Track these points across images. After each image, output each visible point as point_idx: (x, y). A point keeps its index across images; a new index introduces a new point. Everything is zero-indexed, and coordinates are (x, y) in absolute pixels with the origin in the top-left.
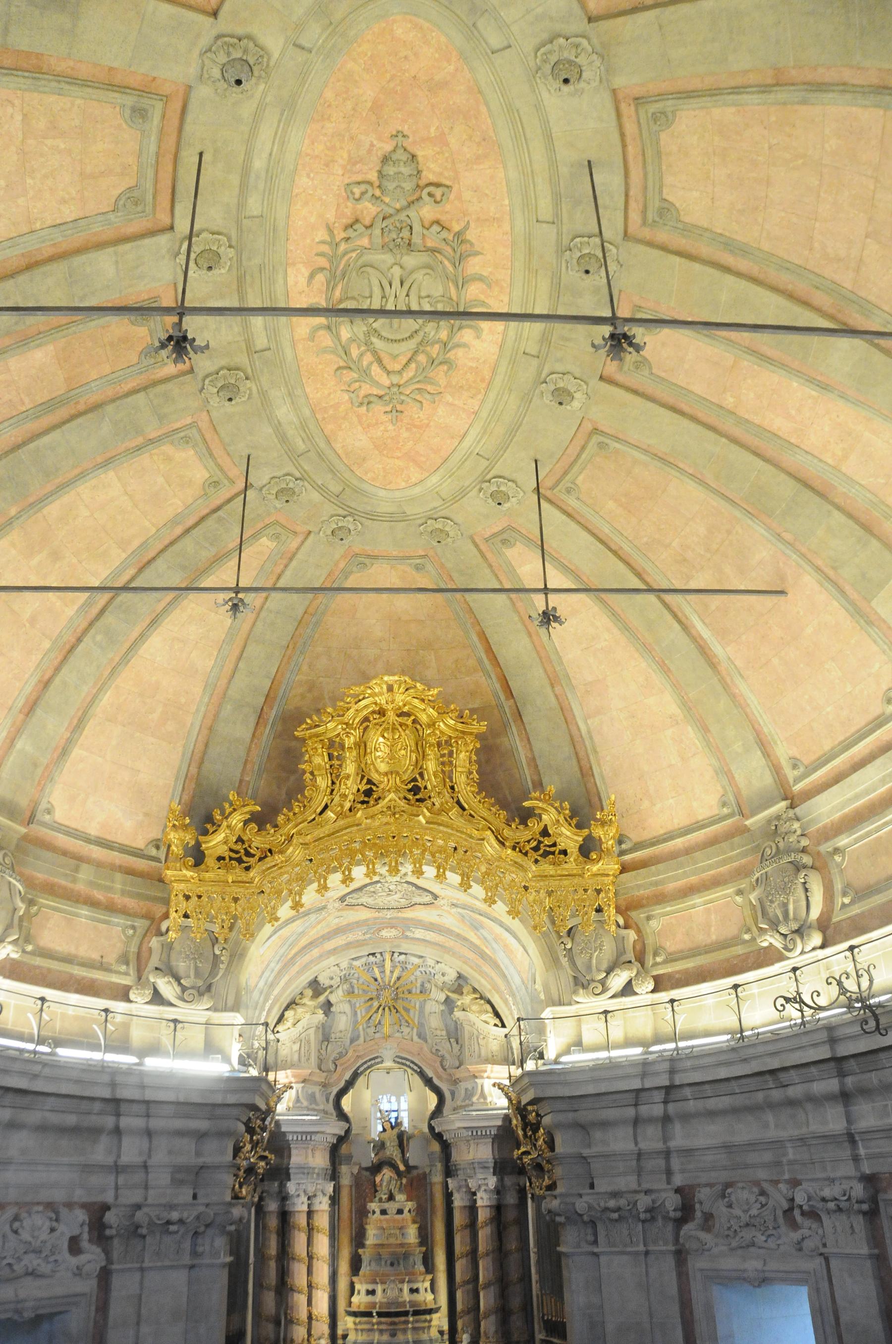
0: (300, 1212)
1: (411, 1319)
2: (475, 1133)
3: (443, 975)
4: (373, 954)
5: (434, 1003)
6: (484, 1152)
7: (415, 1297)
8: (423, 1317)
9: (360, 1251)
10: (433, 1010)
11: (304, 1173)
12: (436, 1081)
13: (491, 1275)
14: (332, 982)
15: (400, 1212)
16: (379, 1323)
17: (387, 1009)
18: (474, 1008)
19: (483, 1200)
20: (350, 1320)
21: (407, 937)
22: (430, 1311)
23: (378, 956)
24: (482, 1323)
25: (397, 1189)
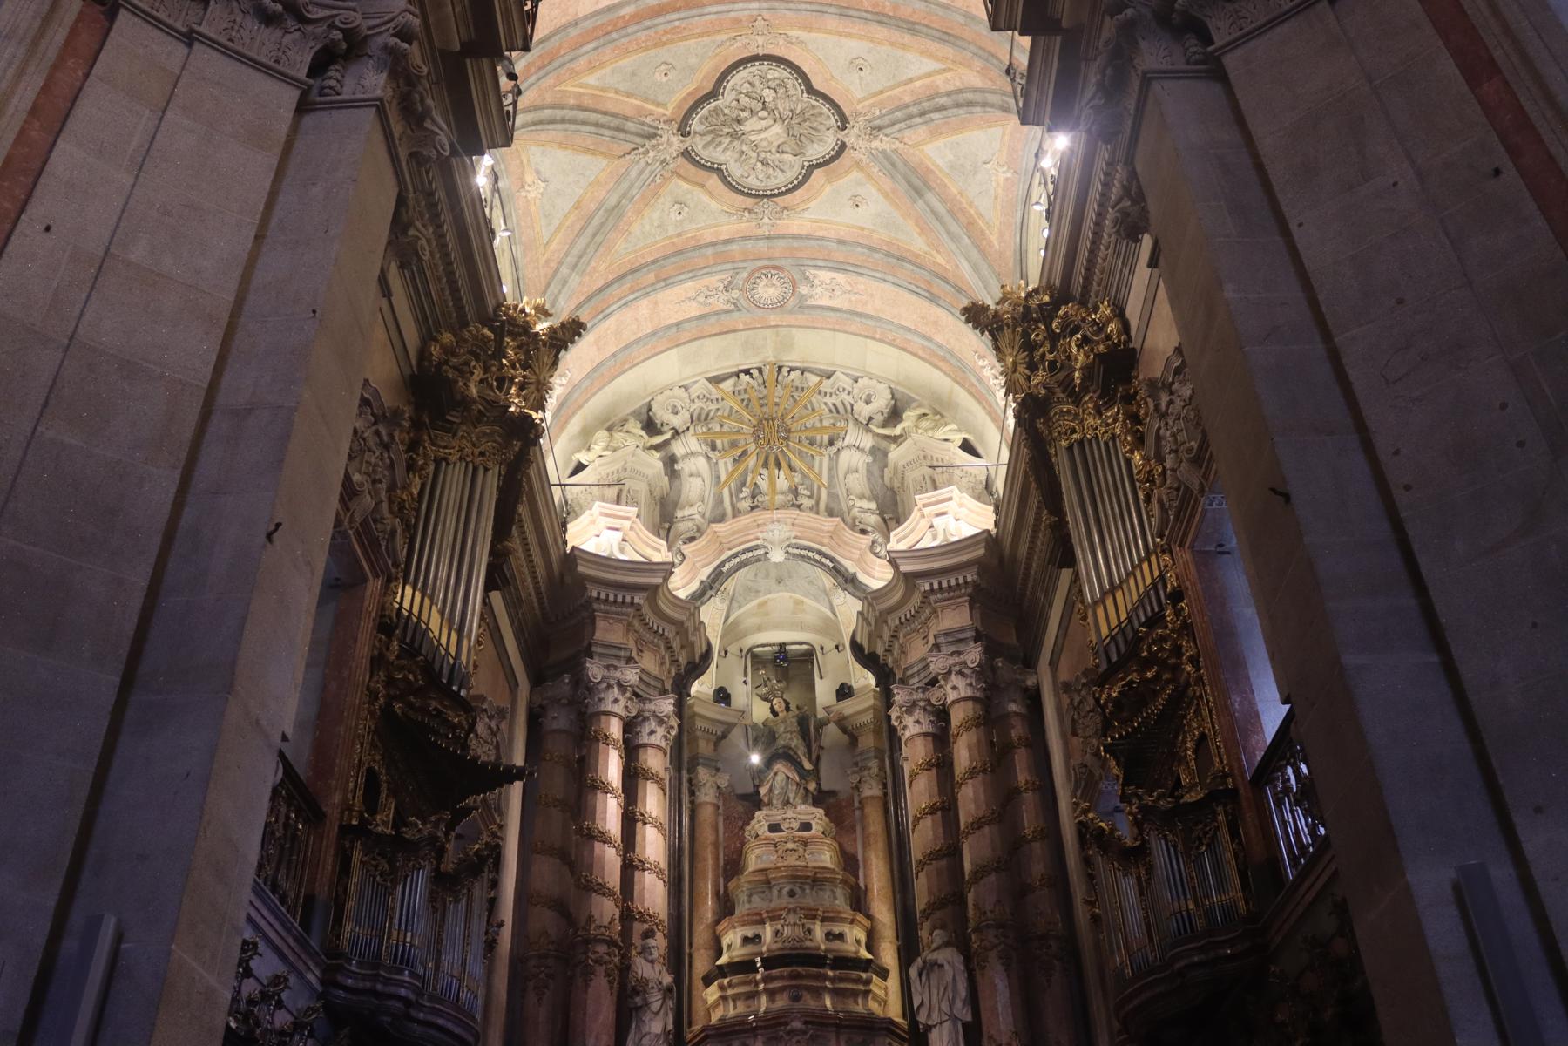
0: (608, 714)
1: (830, 973)
2: (936, 586)
3: (868, 402)
4: (747, 372)
5: (853, 450)
6: (957, 617)
7: (837, 945)
8: (854, 974)
9: (731, 885)
10: (854, 465)
11: (618, 657)
12: (862, 578)
13: (984, 807)
14: (677, 421)
15: (806, 826)
16: (765, 980)
17: (772, 460)
18: (924, 424)
19: (957, 690)
20: (712, 994)
21: (802, 307)
22: (866, 965)
23: (755, 373)
24: (970, 897)
25: (798, 800)
